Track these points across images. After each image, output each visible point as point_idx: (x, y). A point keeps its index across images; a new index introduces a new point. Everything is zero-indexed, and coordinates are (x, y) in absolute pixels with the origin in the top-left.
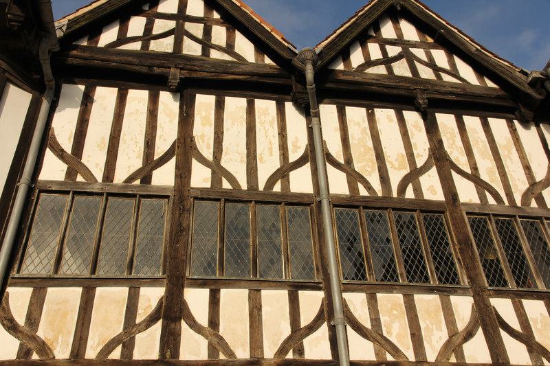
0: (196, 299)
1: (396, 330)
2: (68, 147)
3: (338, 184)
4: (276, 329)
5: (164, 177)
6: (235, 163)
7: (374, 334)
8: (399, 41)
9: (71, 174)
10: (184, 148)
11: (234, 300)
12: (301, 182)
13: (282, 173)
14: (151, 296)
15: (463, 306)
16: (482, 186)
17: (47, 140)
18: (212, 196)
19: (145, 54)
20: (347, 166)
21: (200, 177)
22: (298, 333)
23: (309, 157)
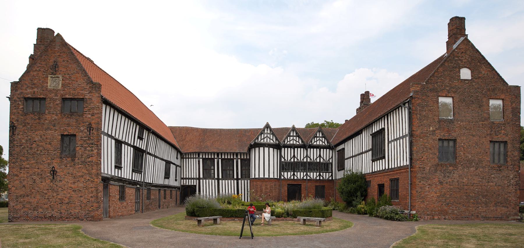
0: (296, 173)
1: (312, 176)
3: (309, 160)
5: (292, 160)
6: (299, 158)
7: (310, 176)
8: (319, 137)
10: (294, 156)
11: (299, 173)
12: (305, 160)
13: (303, 159)
14: (292, 173)
15: (318, 174)
16: (324, 159)
18: (297, 162)
19: (290, 144)
20: (310, 158)
22: (304, 176)
23: (306, 157)
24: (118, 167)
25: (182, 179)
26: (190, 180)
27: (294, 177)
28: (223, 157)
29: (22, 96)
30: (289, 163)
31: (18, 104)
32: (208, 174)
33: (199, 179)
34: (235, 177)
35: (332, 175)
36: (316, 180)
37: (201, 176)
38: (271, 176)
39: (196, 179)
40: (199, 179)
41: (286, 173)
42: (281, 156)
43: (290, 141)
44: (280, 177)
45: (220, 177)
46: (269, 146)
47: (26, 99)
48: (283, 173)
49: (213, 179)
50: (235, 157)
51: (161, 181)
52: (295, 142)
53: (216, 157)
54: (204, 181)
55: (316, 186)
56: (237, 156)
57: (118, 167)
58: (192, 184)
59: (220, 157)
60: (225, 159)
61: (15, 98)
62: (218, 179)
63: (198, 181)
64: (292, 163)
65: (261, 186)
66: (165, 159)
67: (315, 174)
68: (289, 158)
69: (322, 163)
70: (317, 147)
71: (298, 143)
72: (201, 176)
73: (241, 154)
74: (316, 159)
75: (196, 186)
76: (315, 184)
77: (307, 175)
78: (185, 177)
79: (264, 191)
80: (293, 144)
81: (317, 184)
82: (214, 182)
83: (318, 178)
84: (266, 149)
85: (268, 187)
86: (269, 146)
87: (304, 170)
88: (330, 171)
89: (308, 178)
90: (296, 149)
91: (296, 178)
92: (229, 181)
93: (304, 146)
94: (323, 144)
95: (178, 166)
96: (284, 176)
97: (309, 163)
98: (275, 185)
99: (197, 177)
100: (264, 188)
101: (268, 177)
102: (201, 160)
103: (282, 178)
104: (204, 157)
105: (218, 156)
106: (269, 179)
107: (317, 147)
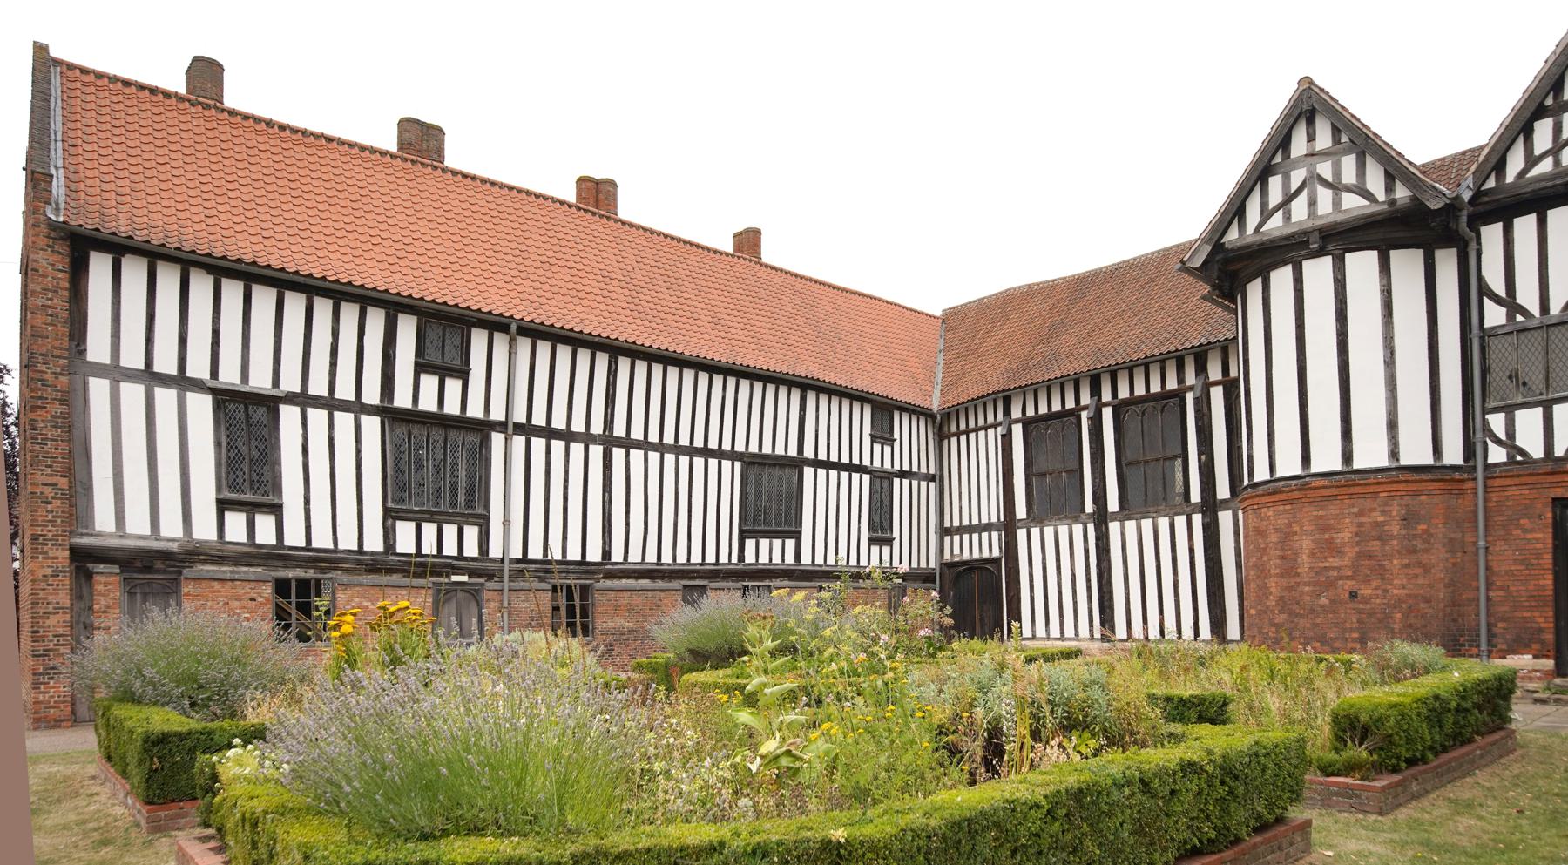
2: (1502, 292)
9: (1510, 317)
17: (1485, 291)
26: (956, 538)
28: (1123, 393)
33: (1008, 526)
34: (1196, 496)
37: (1021, 512)
38: (1371, 453)
40: (1008, 526)
42: (1472, 291)
45: (1113, 505)
46: (1337, 239)
48: (1497, 422)
49: (1076, 520)
50: (1190, 379)
54: (1035, 532)
56: (1201, 369)
58: (986, 554)
59: (1106, 396)
60: (1133, 401)
65: (1286, 536)
72: (1021, 512)
79: (1305, 565)
82: (1079, 535)
84: (1318, 272)
85: (1345, 535)
86: (1337, 239)
92: (1163, 523)
96: (1509, 443)
98: (1408, 520)
100: (1305, 544)
102: (1017, 430)
105: (1096, 391)
106: (1351, 482)
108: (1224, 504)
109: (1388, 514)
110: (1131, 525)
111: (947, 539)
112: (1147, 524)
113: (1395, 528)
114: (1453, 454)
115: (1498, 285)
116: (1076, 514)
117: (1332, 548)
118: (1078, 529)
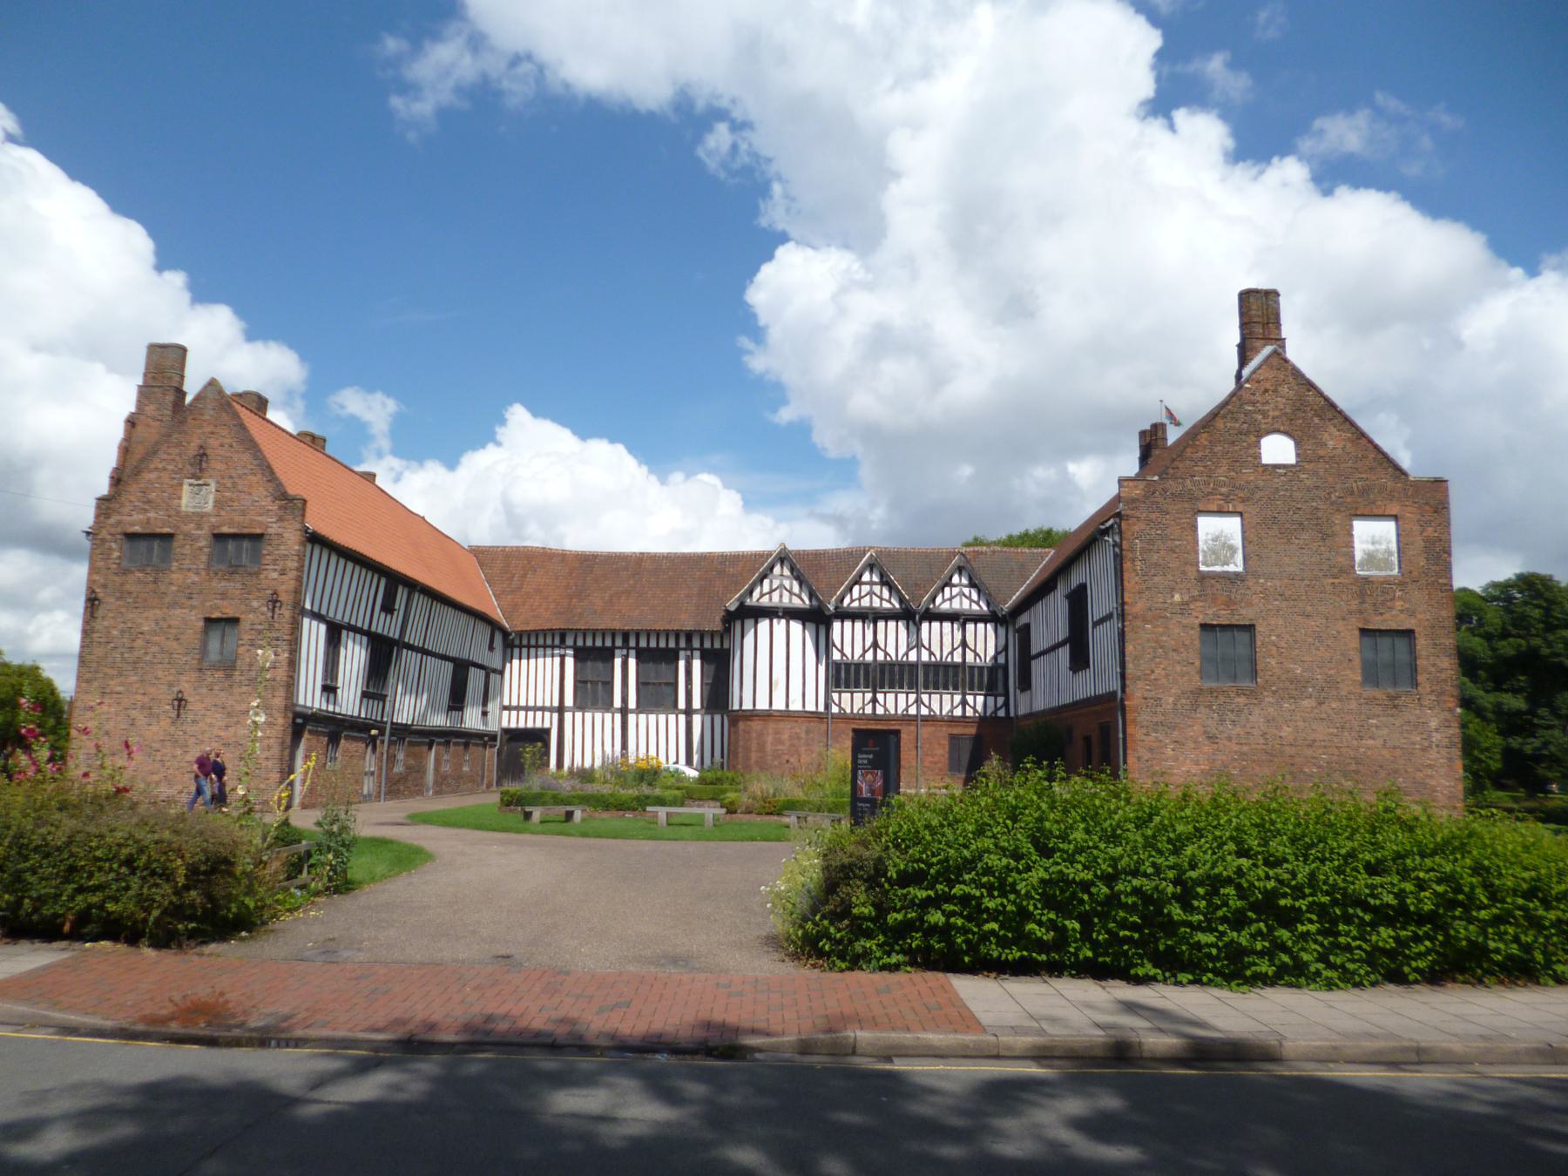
0: (880, 697)
1: (936, 707)
3: (925, 657)
4: (902, 706)
6: (891, 651)
7: (929, 707)
10: (875, 645)
11: (891, 697)
12: (913, 657)
14: (869, 696)
15: (958, 698)
18: (883, 665)
19: (860, 607)
20: (929, 649)
21: (881, 656)
24: (329, 689)
25: (505, 708)
27: (874, 708)
29: (119, 530)
30: (858, 665)
31: (110, 549)
32: (593, 693)
33: (561, 709)
35: (1006, 704)
36: (952, 720)
38: (796, 706)
39: (551, 710)
40: (561, 709)
41: (846, 696)
43: (860, 598)
44: (827, 706)
45: (632, 704)
47: (131, 537)
48: (835, 696)
51: (439, 720)
52: (876, 603)
53: (619, 643)
55: (953, 737)
57: (329, 689)
60: (648, 649)
61: (104, 534)
62: (624, 711)
63: (556, 716)
64: (867, 665)
65: (760, 735)
66: (453, 654)
67: (946, 698)
68: (858, 651)
69: (972, 668)
70: (952, 617)
71: (886, 605)
73: (702, 635)
74: (951, 653)
75: (547, 732)
76: (945, 731)
77: (918, 701)
78: (514, 703)
79: (769, 748)
80: (871, 608)
81: (956, 731)
82: (611, 721)
83: (958, 712)
85: (785, 736)
87: (913, 685)
88: (1000, 689)
89: (924, 711)
90: (881, 624)
91: (880, 711)
93: (910, 616)
94: (975, 607)
95: (494, 671)
97: (927, 666)
98: (807, 732)
99: (556, 703)
100: (770, 739)
101: (783, 707)
103: (835, 709)
104: (580, 643)
106: (787, 715)
107: (952, 617)
108: (696, 711)
109: (801, 728)
110: (642, 717)
111: (506, 713)
112: (652, 717)
113: (803, 735)
114: (821, 709)
115: (838, 644)
116: (608, 706)
117: (780, 742)
118: (608, 716)
